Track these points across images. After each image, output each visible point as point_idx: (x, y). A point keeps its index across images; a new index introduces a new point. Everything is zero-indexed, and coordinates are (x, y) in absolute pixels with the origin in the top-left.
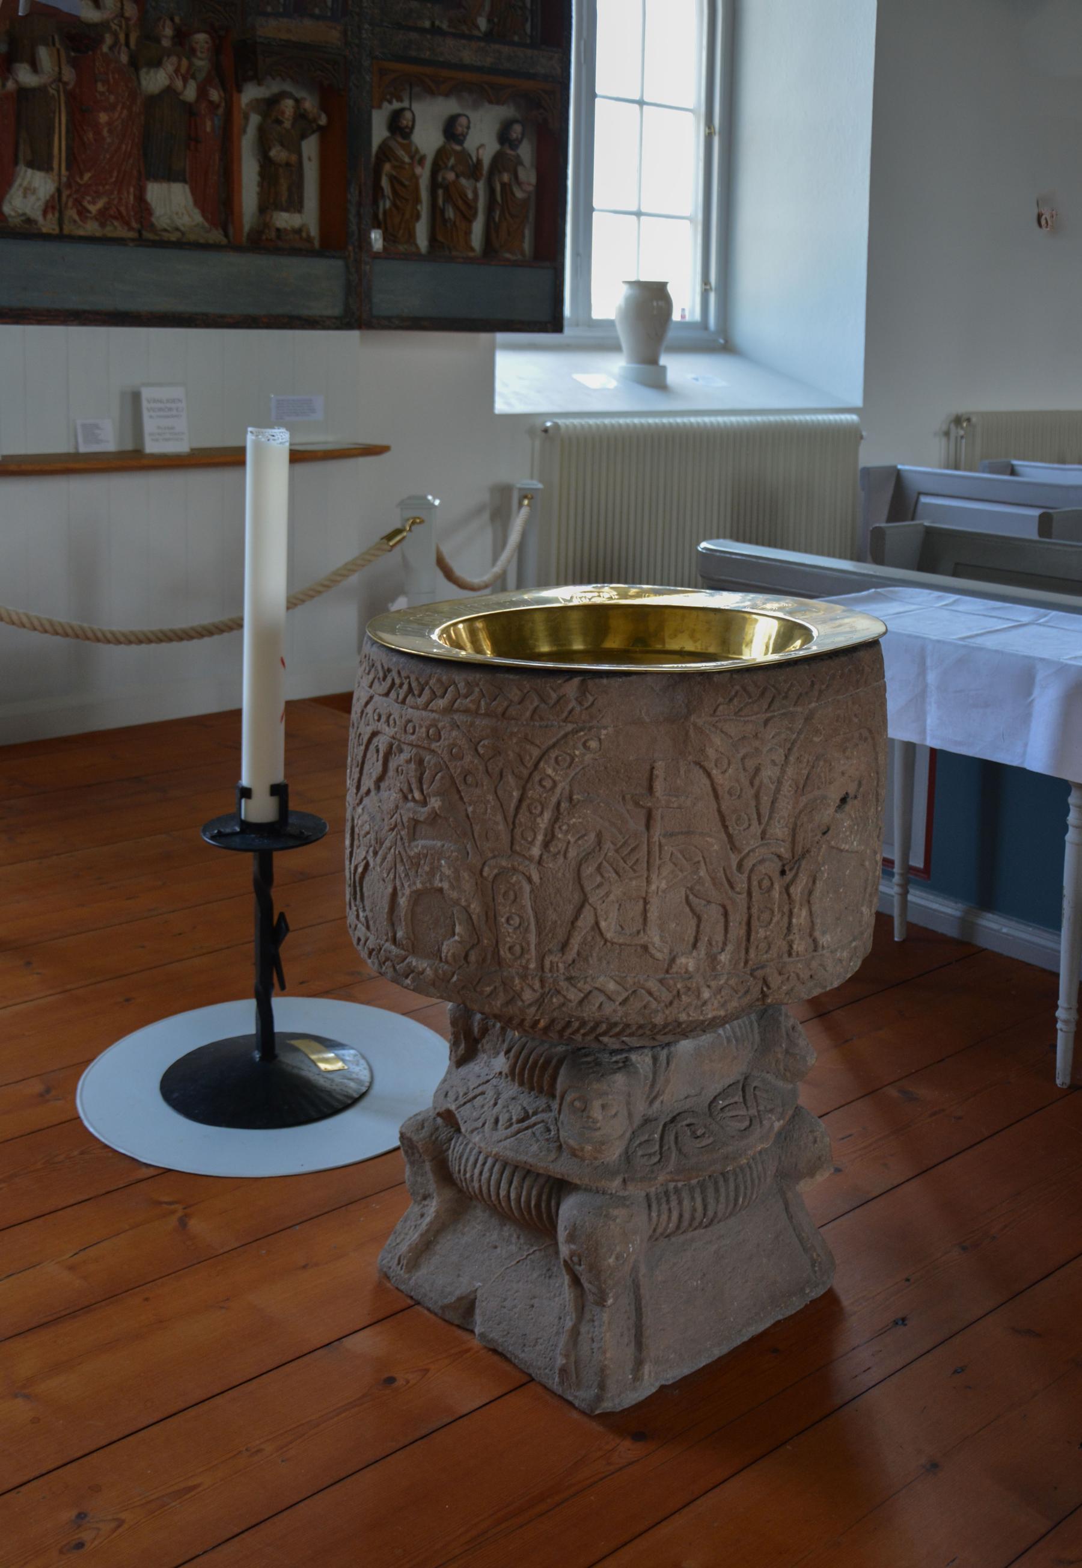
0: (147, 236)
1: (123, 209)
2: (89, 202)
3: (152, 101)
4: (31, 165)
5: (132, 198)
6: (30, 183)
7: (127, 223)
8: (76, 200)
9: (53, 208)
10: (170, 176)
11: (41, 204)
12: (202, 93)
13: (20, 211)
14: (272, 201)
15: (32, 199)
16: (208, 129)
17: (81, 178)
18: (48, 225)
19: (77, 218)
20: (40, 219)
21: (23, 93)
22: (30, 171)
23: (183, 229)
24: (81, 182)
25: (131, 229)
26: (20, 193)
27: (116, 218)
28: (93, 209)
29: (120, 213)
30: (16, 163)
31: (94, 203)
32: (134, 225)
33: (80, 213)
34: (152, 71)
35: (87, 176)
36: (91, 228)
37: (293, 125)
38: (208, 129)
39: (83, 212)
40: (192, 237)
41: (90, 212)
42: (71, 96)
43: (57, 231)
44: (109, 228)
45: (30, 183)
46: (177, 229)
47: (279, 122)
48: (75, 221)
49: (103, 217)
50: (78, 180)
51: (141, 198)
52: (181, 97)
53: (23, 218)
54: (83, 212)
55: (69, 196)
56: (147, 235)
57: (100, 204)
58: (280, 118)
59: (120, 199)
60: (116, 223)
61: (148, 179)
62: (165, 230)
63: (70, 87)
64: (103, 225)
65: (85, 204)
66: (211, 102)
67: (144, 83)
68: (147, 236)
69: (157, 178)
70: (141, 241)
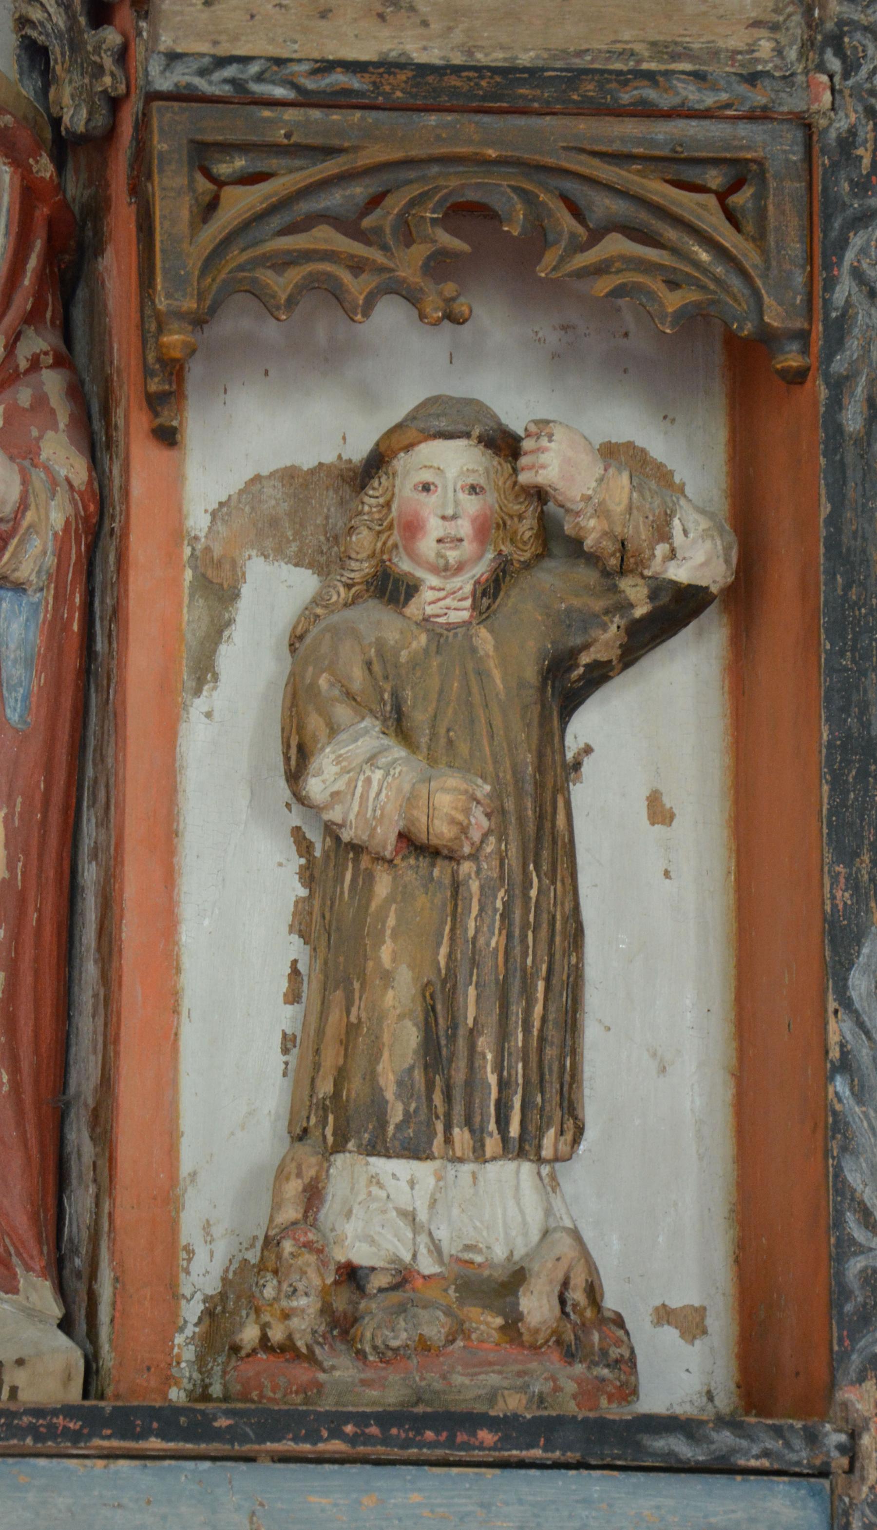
14: (325, 1088)
37: (490, 592)
47: (391, 588)
58: (405, 565)
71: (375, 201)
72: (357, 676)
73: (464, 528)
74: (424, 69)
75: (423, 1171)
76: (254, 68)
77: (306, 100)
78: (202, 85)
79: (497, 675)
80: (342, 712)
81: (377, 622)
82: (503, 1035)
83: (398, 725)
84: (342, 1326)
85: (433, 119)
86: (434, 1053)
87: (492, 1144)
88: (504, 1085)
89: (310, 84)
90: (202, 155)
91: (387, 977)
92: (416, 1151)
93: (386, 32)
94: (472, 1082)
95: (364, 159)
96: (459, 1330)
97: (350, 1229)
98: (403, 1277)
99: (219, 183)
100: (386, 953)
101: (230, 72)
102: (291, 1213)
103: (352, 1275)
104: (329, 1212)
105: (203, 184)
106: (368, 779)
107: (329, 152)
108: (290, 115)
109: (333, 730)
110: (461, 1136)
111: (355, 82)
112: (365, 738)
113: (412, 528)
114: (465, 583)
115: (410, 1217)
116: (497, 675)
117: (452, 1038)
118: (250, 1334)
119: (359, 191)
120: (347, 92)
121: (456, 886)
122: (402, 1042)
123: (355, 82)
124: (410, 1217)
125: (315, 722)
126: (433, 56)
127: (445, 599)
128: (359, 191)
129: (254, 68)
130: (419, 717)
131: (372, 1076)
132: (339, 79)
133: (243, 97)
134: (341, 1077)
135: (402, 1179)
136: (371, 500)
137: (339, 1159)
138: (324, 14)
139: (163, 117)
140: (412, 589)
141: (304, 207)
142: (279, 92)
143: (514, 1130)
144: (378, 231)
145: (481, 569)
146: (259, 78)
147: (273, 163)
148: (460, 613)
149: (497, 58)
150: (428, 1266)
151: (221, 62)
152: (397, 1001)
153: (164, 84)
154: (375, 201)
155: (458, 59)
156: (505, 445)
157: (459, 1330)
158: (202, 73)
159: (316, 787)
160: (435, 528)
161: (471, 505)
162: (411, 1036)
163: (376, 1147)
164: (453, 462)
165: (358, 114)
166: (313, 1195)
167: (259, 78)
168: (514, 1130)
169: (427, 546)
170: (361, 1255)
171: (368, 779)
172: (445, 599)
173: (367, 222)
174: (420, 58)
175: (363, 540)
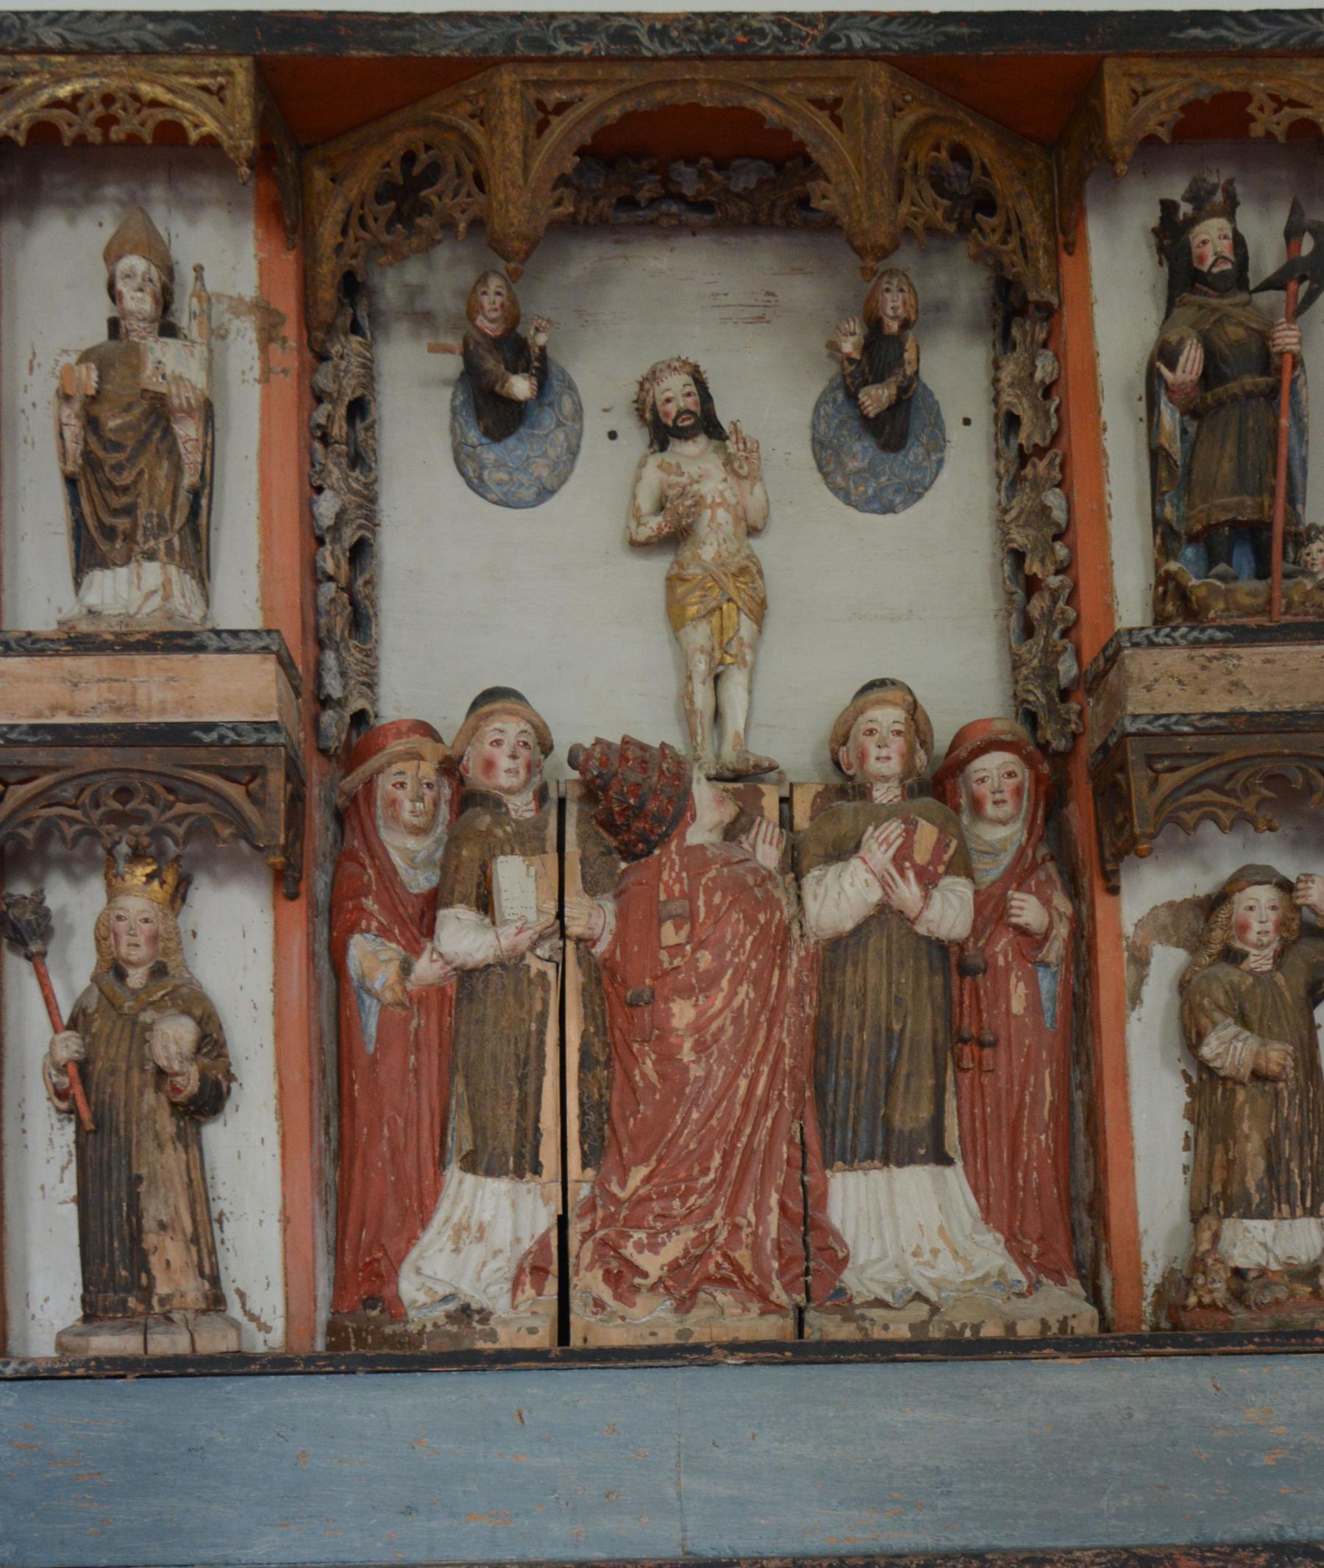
0: (817, 1326)
1: (743, 1256)
2: (640, 1247)
3: (839, 950)
4: (471, 1164)
5: (773, 1218)
6: (469, 1211)
7: (763, 1296)
8: (604, 1242)
9: (539, 1272)
10: (894, 1152)
11: (503, 1266)
12: (991, 910)
13: (442, 1290)
14: (1217, 1189)
15: (475, 1253)
16: (1017, 1006)
17: (623, 1185)
18: (522, 1320)
19: (606, 1294)
20: (501, 1305)
21: (466, 975)
22: (469, 1178)
23: (932, 1294)
24: (622, 1195)
25: (769, 1307)
26: (446, 1242)
27: (725, 1282)
28: (653, 1264)
29: (737, 1268)
30: (441, 1164)
31: (654, 1247)
32: (778, 1294)
33: (613, 1279)
34: (833, 870)
35: (638, 1174)
36: (651, 1319)
37: (1279, 957)
38: (1017, 1006)
39: (622, 1278)
40: (961, 1317)
41: (645, 1275)
42: (603, 977)
43: (544, 1337)
44: (698, 1313)
45: (469, 1211)
46: (919, 1297)
47: (1232, 956)
48: (599, 1304)
49: (684, 1284)
50: (614, 1188)
51: (807, 1219)
52: (921, 929)
53: (451, 1307)
54: (622, 1278)
55: (586, 1236)
56: (825, 1326)
57: (673, 1248)
58: (1238, 945)
59: (736, 1228)
60: (723, 1297)
61: (828, 1164)
62: (879, 1303)
63: (600, 949)
64: (684, 1306)
65: (629, 1251)
66: (1022, 931)
67: (811, 905)
68: (817, 1326)
69: (851, 1157)
70: (800, 1351)
71: (1230, 777)
72: (1221, 998)
73: (1270, 926)
74: (1253, 714)
75: (1269, 1225)
76: (1174, 719)
77: (1199, 732)
78: (1150, 728)
79: (1287, 995)
80: (1218, 1016)
81: (1229, 974)
82: (1302, 1161)
83: (1243, 1020)
84: (1238, 1296)
85: (1258, 737)
86: (1271, 1171)
87: (1299, 1211)
88: (1303, 1183)
89: (1200, 724)
90: (1150, 760)
91: (1247, 1137)
92: (1265, 1215)
93: (1232, 698)
94: (1289, 1183)
95: (1227, 758)
96: (1292, 1295)
97: (1236, 1252)
98: (1263, 1272)
99: (1157, 772)
100: (1245, 1126)
102: (1205, 1246)
103: (1238, 1273)
104: (1224, 1245)
105: (1151, 774)
106: (1229, 1047)
107: (1209, 755)
108: (1191, 739)
109: (1215, 1024)
110: (1285, 1207)
111: (1221, 722)
112: (1230, 1029)
113: (1243, 928)
114: (1269, 952)
115: (1264, 1245)
116: (1287, 995)
117: (1279, 1163)
118: (1192, 1300)
119: (1224, 772)
120: (1218, 727)
121: (1277, 1094)
122: (1255, 1169)
123: (1221, 722)
124: (1264, 1245)
125: (1204, 1021)
126: (1255, 708)
127: (1260, 960)
128: (1224, 772)
129: (1174, 719)
130: (1254, 1017)
131: (1243, 1183)
132: (1214, 721)
133: (1169, 733)
134: (1226, 1184)
135: (1260, 1228)
136: (1222, 915)
137: (1227, 1222)
138: (1203, 692)
140: (1245, 956)
141: (1198, 781)
142: (1186, 729)
143: (1308, 1204)
144: (1234, 790)
145: (1275, 945)
146: (1176, 723)
147: (1183, 762)
148: (1267, 966)
149: (1285, 707)
150: (1274, 1266)
151: (1158, 717)
152: (1252, 1147)
154: (1230, 777)
155: (1267, 709)
156: (1286, 887)
157: (1292, 1295)
159: (1207, 1051)
160: (1256, 927)
161: (1273, 916)
162: (1261, 1164)
163: (1248, 1215)
164: (1263, 896)
165: (1222, 738)
166: (1216, 1238)
167: (1176, 723)
168: (1308, 1204)
169: (1252, 936)
170: (1241, 1263)
171: (1229, 1047)
172: (1260, 960)
173: (1228, 787)
174: (1249, 709)
175: (1218, 934)
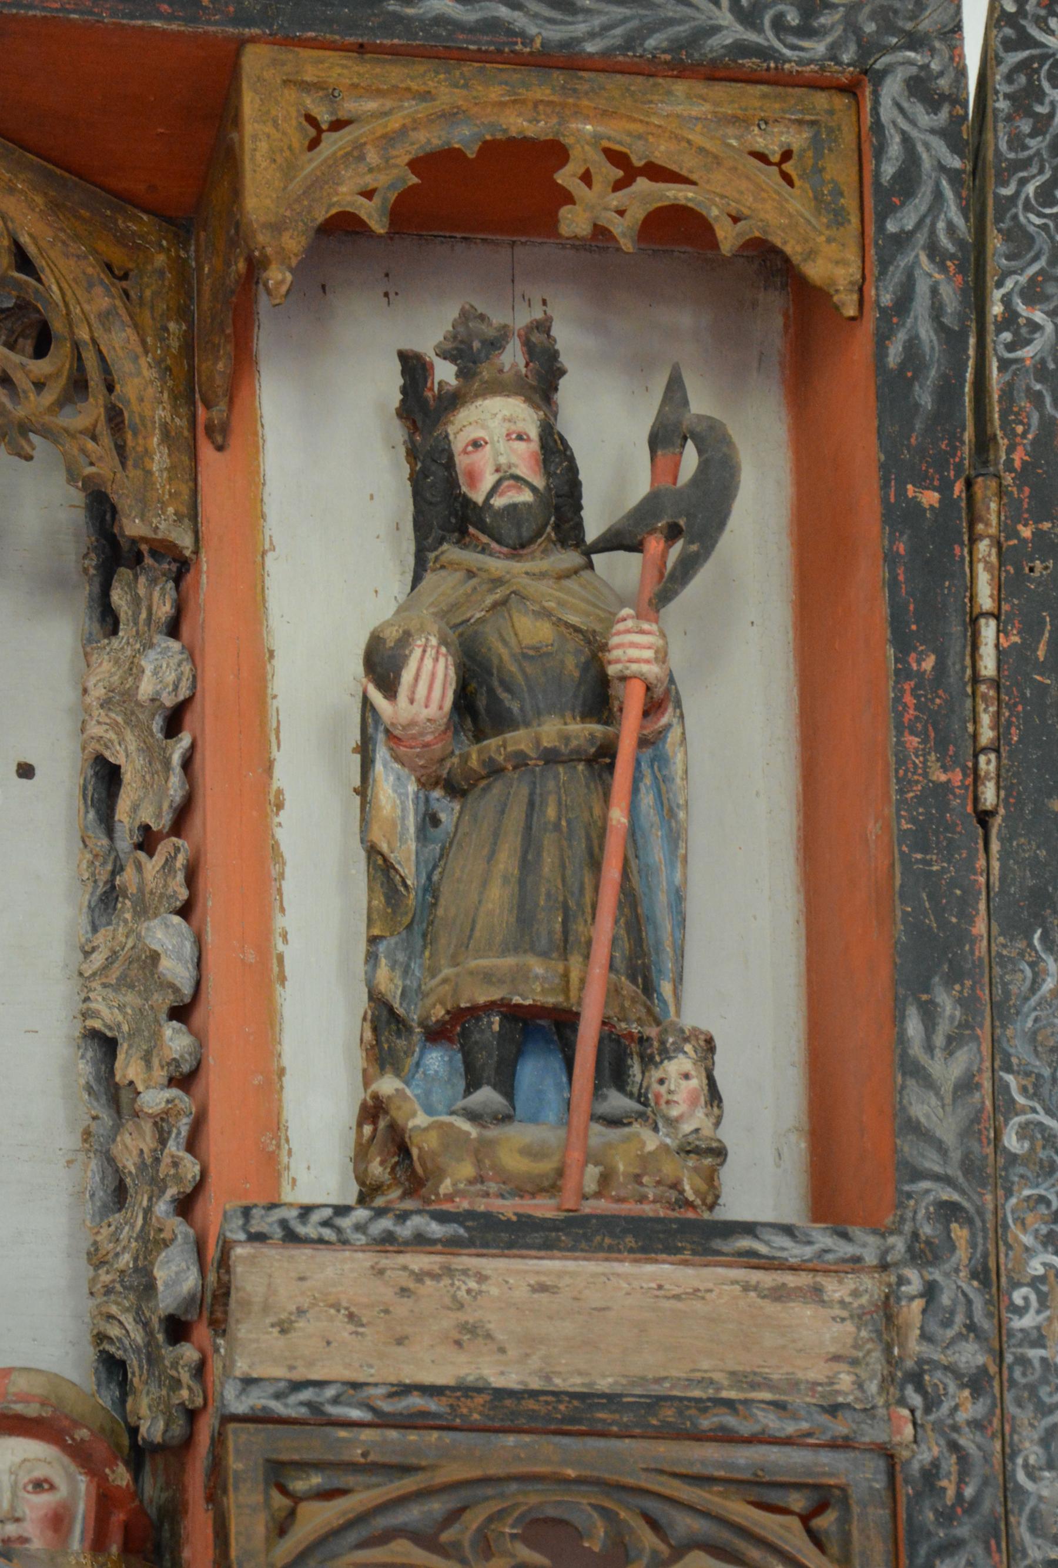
71: (453, 1517)
74: (500, 1394)
76: (330, 1392)
77: (383, 1421)
78: (278, 1407)
85: (511, 1440)
89: (387, 1406)
90: (277, 1473)
93: (462, 1358)
101: (306, 1395)
105: (279, 1501)
107: (406, 1470)
108: (367, 1435)
111: (433, 1405)
119: (437, 1507)
120: (424, 1414)
123: (433, 1405)
126: (511, 1380)
128: (437, 1507)
129: (330, 1392)
132: (416, 1402)
133: (319, 1419)
138: (400, 1341)
139: (237, 1437)
141: (382, 1522)
142: (356, 1414)
144: (456, 1545)
146: (336, 1401)
147: (348, 1480)
149: (574, 1383)
151: (297, 1386)
153: (240, 1407)
154: (453, 1517)
155: (535, 1384)
158: (278, 1396)
165: (435, 1435)
167: (336, 1401)
173: (445, 1537)
174: (498, 1382)
